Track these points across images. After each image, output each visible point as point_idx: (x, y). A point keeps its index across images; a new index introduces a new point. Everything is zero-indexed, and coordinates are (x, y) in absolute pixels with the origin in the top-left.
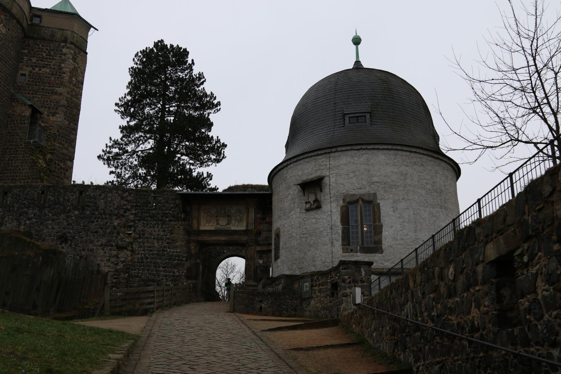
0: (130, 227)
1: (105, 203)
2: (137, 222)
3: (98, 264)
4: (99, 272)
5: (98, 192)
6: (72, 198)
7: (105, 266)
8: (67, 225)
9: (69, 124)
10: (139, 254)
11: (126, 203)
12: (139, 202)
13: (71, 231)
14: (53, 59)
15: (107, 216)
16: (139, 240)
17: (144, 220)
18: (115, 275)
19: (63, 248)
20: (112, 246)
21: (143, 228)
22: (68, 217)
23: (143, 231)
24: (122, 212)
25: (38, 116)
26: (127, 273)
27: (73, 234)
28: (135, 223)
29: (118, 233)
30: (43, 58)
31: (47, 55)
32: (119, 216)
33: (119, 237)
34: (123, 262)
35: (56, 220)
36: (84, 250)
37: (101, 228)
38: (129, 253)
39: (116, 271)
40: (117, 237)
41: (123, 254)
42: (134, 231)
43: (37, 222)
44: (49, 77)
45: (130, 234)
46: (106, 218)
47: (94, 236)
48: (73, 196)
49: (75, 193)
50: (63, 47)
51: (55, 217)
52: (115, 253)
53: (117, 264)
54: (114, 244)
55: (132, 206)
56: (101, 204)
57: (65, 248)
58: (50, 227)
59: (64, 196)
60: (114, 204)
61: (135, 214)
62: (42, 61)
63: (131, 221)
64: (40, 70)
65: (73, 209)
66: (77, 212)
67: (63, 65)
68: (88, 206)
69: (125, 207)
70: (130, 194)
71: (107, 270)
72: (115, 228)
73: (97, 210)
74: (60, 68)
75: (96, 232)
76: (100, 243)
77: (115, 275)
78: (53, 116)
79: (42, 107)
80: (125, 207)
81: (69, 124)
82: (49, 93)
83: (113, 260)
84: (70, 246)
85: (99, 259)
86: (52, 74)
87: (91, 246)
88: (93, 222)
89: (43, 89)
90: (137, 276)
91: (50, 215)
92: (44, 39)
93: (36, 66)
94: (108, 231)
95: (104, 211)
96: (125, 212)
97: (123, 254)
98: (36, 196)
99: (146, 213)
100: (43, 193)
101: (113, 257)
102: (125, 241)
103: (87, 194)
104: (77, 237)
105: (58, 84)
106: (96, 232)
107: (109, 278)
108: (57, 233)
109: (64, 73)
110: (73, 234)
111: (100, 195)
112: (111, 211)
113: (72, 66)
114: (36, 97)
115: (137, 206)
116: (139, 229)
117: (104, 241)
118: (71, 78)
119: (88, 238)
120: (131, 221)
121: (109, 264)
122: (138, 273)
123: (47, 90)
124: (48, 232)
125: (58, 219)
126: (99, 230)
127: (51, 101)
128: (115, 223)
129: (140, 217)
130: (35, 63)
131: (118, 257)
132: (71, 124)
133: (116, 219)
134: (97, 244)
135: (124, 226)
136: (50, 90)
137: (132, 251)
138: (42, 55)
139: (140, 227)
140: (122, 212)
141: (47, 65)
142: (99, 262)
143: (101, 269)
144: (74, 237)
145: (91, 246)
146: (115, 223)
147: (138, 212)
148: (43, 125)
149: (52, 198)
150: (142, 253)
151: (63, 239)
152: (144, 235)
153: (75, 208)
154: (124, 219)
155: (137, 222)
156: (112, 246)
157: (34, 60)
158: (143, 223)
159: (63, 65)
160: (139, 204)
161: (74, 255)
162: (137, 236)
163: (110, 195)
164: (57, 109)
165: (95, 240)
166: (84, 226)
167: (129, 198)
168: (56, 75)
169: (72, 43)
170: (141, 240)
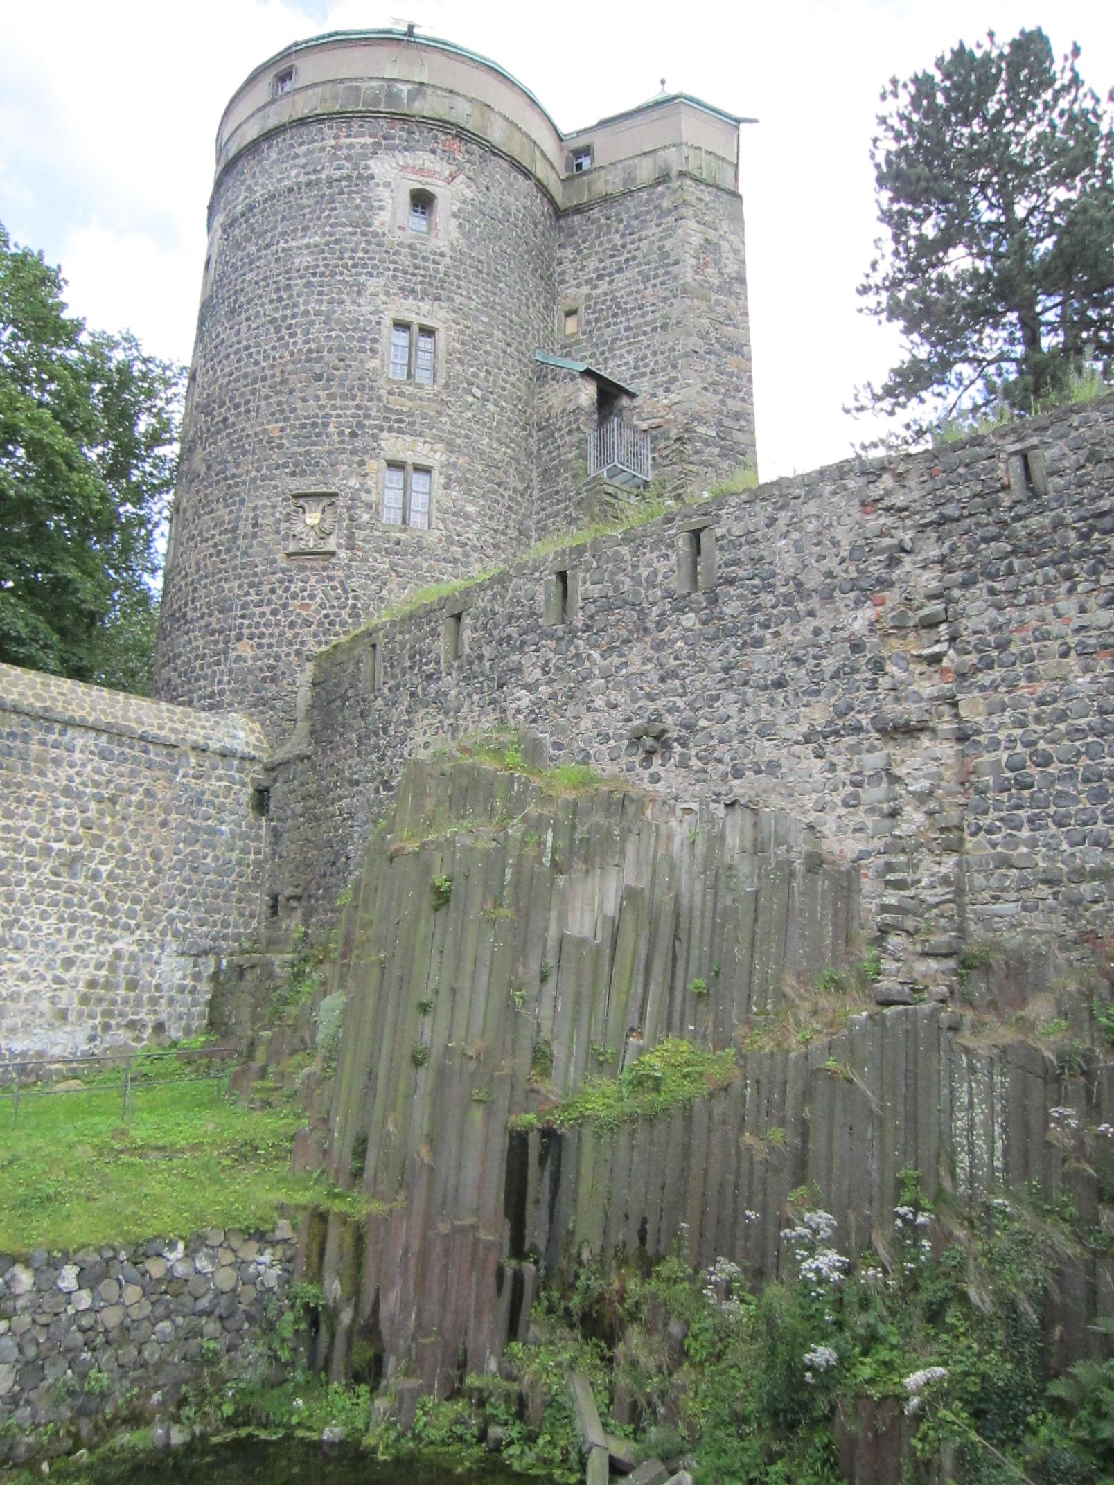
0: (930, 624)
1: (798, 547)
2: (956, 593)
3: (811, 827)
4: (815, 862)
5: (762, 511)
6: (662, 567)
7: (840, 830)
8: (662, 679)
9: (723, 402)
10: (996, 744)
11: (890, 521)
12: (950, 500)
13: (680, 703)
14: (640, 239)
15: (815, 602)
16: (983, 678)
17: (992, 576)
18: (890, 867)
19: (655, 779)
20: (858, 729)
21: (992, 613)
22: (659, 646)
23: (996, 628)
24: (875, 568)
25: (625, 401)
26: (950, 849)
27: (688, 714)
28: (950, 601)
29: (878, 666)
30: (614, 248)
31: (623, 236)
32: (867, 591)
33: (884, 682)
34: (922, 798)
35: (618, 669)
36: (738, 774)
37: (799, 661)
38: (947, 750)
39: (897, 846)
40: (874, 685)
41: (916, 762)
42: (953, 639)
43: (554, 696)
44: (638, 292)
45: (935, 659)
46: (811, 614)
47: (772, 702)
48: (666, 557)
49: (671, 546)
50: (662, 196)
51: (615, 660)
52: (872, 762)
53: (894, 814)
54: (864, 720)
55: (922, 528)
56: (783, 555)
57: (668, 778)
58: (600, 702)
59: (635, 567)
60: (836, 544)
61: (942, 561)
62: (612, 256)
63: (931, 597)
64: (610, 283)
65: (674, 610)
66: (689, 620)
67: (668, 244)
68: (731, 582)
69: (887, 541)
70: (900, 477)
71: (851, 846)
72: (857, 647)
73: (769, 588)
74: (664, 255)
75: (780, 684)
76: (803, 728)
77: (890, 867)
78: (667, 390)
79: (633, 377)
80: (887, 541)
81: (723, 402)
82: (645, 333)
83: (874, 794)
84: (683, 764)
85: (809, 801)
86: (646, 279)
87: (767, 750)
88: (759, 642)
89: (628, 329)
90: (1005, 862)
91: (596, 655)
92: (607, 200)
93: (600, 277)
94: (830, 664)
95: (799, 585)
96: (893, 563)
97: (916, 762)
98: (540, 598)
99: (996, 538)
100: (562, 576)
101: (875, 779)
102: (919, 698)
103: (719, 532)
104: (703, 723)
105: (665, 299)
106: (780, 684)
107: (867, 885)
108: (629, 720)
109: (676, 263)
110: (688, 714)
111: (771, 522)
112: (830, 575)
113: (696, 240)
114: (614, 357)
115: (943, 520)
116: (972, 624)
117: (818, 714)
118: (698, 269)
119: (749, 716)
120: (931, 597)
121: (860, 816)
122: (1012, 842)
123: (638, 326)
124: (597, 724)
125: (625, 664)
126: (791, 671)
127: (654, 354)
128: (857, 625)
129: (969, 566)
130: (597, 270)
131: (895, 780)
132: (729, 402)
133: (858, 604)
134: (789, 733)
135: (900, 627)
136: (647, 324)
137: (962, 737)
138: (610, 241)
139: (977, 612)
140: (875, 568)
141: (627, 260)
142: (812, 817)
143: (825, 846)
144: (690, 727)
145: (767, 750)
146: (857, 625)
147: (953, 549)
148: (645, 425)
149: (595, 591)
150: (1011, 740)
151: (652, 742)
152: (1002, 646)
153: (680, 604)
154: (892, 597)
155: (956, 593)
156: (858, 729)
157: (592, 264)
158: (992, 592)
159: (668, 244)
160: (951, 510)
161: (703, 802)
162: (973, 658)
163: (812, 508)
164: (674, 367)
165: (781, 721)
166: (726, 670)
167: (900, 500)
168: (656, 277)
169: (682, 174)
170: (997, 673)
